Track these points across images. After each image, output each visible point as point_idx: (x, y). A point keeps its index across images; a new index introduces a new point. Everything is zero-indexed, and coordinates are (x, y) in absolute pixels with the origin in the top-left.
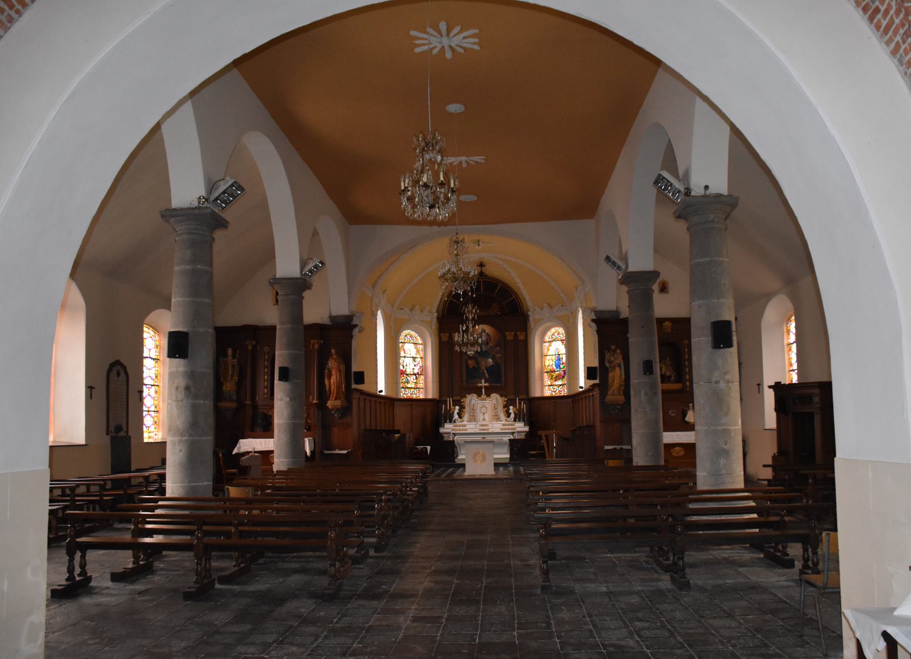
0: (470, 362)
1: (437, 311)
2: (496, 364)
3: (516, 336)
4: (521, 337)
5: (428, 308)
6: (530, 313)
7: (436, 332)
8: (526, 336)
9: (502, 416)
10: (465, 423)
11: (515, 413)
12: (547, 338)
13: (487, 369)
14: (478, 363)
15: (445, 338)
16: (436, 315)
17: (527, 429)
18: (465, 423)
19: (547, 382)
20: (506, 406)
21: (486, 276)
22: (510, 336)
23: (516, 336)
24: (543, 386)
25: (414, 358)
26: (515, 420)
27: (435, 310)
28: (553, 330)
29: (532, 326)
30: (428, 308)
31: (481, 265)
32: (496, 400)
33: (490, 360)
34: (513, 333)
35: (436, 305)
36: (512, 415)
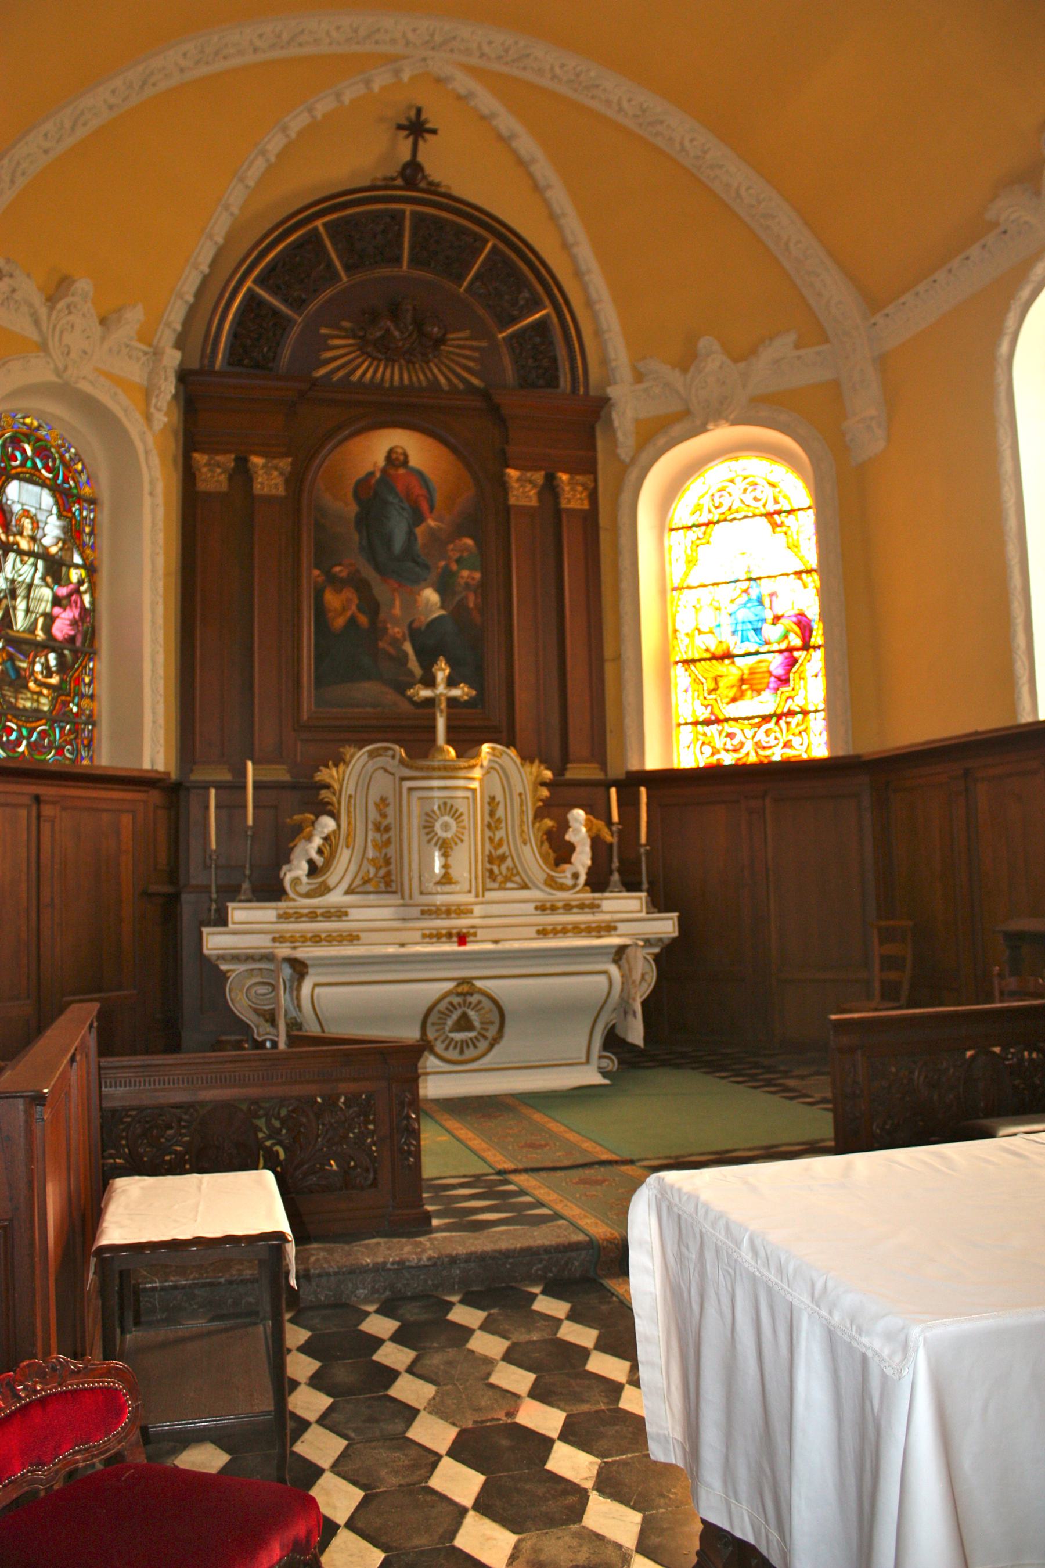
0: (332, 599)
1: (180, 344)
2: (457, 612)
3: (550, 489)
4: (573, 497)
5: (135, 316)
6: (612, 392)
7: (173, 447)
8: (593, 497)
9: (531, 857)
10: (336, 898)
11: (596, 843)
12: (682, 512)
13: (414, 634)
14: (371, 606)
15: (214, 476)
16: (173, 358)
17: (667, 926)
18: (336, 898)
19: (688, 705)
20: (553, 807)
21: (433, 188)
22: (522, 488)
23: (550, 489)
24: (668, 727)
25: (55, 568)
26: (597, 881)
27: (167, 338)
28: (717, 473)
29: (624, 453)
30: (135, 316)
31: (416, 128)
32: (489, 776)
33: (430, 596)
34: (539, 477)
35: (176, 315)
36: (582, 859)
